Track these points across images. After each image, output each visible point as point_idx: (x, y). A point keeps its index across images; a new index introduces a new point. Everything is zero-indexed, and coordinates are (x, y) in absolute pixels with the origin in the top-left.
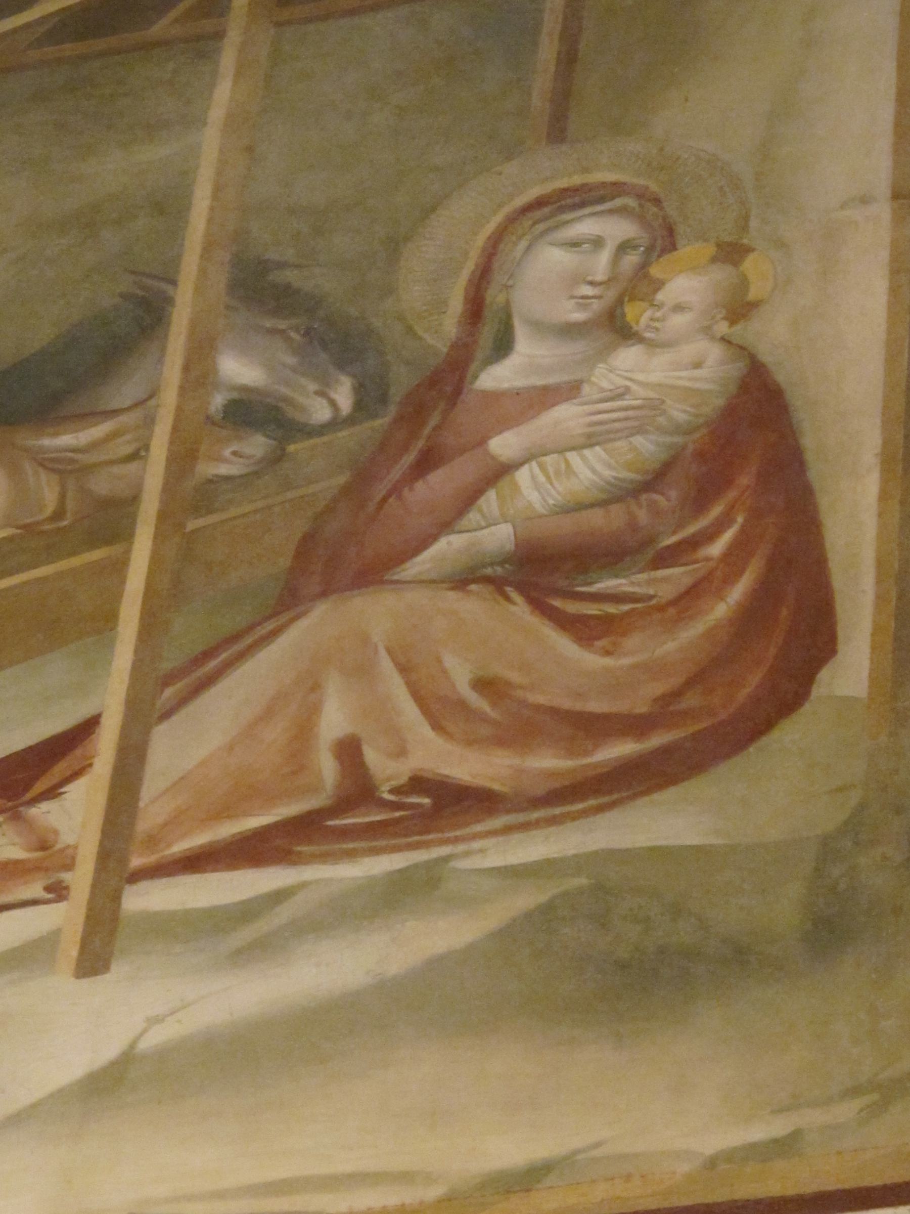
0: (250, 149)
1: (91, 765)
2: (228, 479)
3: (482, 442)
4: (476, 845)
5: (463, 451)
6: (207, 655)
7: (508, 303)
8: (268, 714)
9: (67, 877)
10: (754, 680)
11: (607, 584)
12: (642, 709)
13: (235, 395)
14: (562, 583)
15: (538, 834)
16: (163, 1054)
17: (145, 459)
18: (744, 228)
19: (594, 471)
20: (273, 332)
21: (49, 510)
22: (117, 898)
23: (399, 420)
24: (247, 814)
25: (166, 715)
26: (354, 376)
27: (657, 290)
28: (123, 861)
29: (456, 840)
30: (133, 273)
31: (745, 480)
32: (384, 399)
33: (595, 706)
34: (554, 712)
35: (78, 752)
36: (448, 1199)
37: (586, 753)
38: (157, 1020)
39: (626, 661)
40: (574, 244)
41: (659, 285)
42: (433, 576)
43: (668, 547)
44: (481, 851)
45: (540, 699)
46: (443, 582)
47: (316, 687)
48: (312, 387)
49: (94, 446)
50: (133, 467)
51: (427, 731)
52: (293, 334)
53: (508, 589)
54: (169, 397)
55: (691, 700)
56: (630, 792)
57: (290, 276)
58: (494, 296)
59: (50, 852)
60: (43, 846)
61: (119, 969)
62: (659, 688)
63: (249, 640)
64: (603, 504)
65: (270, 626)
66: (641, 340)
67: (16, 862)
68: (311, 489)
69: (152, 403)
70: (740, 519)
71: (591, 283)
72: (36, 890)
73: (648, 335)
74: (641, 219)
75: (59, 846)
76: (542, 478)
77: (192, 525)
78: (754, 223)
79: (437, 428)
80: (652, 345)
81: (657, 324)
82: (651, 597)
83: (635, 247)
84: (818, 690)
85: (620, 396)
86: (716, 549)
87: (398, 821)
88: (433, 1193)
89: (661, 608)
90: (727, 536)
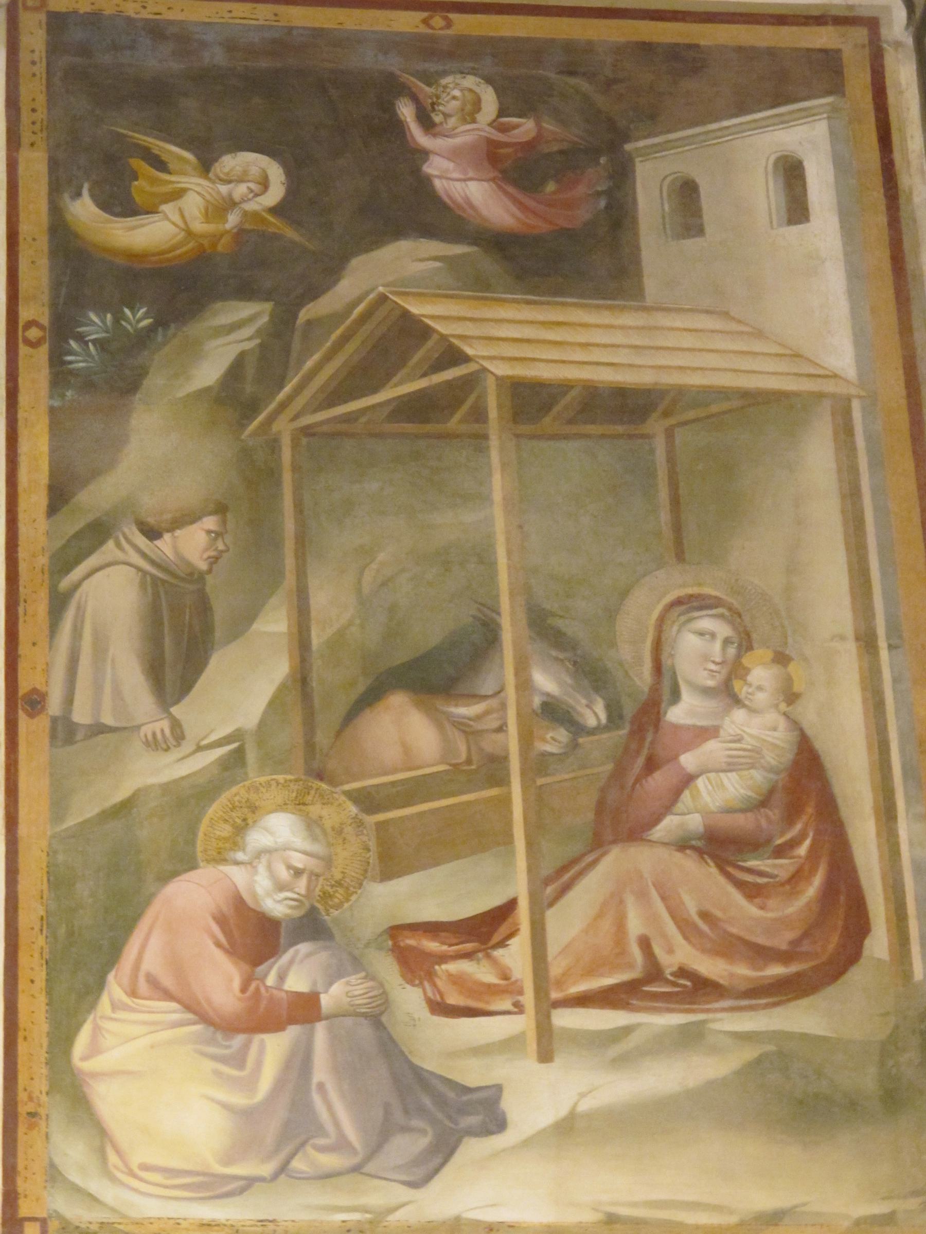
0: (520, 527)
1: (518, 930)
2: (552, 754)
3: (675, 758)
4: (719, 1015)
5: (668, 761)
6: (564, 869)
7: (673, 663)
8: (600, 915)
9: (520, 998)
10: (835, 939)
11: (752, 863)
12: (784, 947)
13: (545, 699)
14: (732, 858)
15: (747, 1015)
16: (589, 1116)
17: (506, 731)
18: (786, 644)
19: (736, 789)
20: (556, 659)
21: (464, 757)
22: (548, 1016)
23: (632, 733)
24: (602, 975)
25: (551, 904)
26: (604, 698)
27: (747, 674)
28: (547, 994)
29: (708, 1011)
30: (476, 602)
31: (810, 810)
32: (621, 717)
33: (761, 940)
34: (740, 939)
35: (510, 920)
36: (741, 1224)
37: (761, 969)
38: (582, 1095)
39: (770, 915)
40: (701, 634)
41: (748, 671)
42: (666, 841)
43: (779, 845)
44: (721, 1020)
45: (734, 930)
46: (673, 845)
47: (621, 902)
48: (584, 701)
49: (478, 718)
50: (500, 737)
51: (683, 942)
52: (567, 663)
53: (706, 856)
54: (511, 693)
55: (806, 947)
56: (785, 998)
57: (559, 623)
58: (666, 662)
59: (510, 981)
60: (506, 977)
61: (558, 1061)
62: (790, 935)
63: (583, 864)
64: (743, 811)
65: (589, 858)
66: (744, 706)
67: (495, 985)
68: (595, 770)
69: (502, 694)
70: (811, 834)
71: (713, 662)
72: (507, 1005)
73: (747, 702)
74: (731, 623)
75: (513, 979)
76: (710, 787)
77: (540, 781)
78: (790, 640)
79: (652, 743)
80: (752, 711)
81: (750, 697)
82: (777, 876)
83: (732, 643)
84: (866, 952)
85: (739, 741)
86: (803, 850)
87: (677, 993)
88: (733, 1220)
89: (782, 884)
90: (807, 843)
